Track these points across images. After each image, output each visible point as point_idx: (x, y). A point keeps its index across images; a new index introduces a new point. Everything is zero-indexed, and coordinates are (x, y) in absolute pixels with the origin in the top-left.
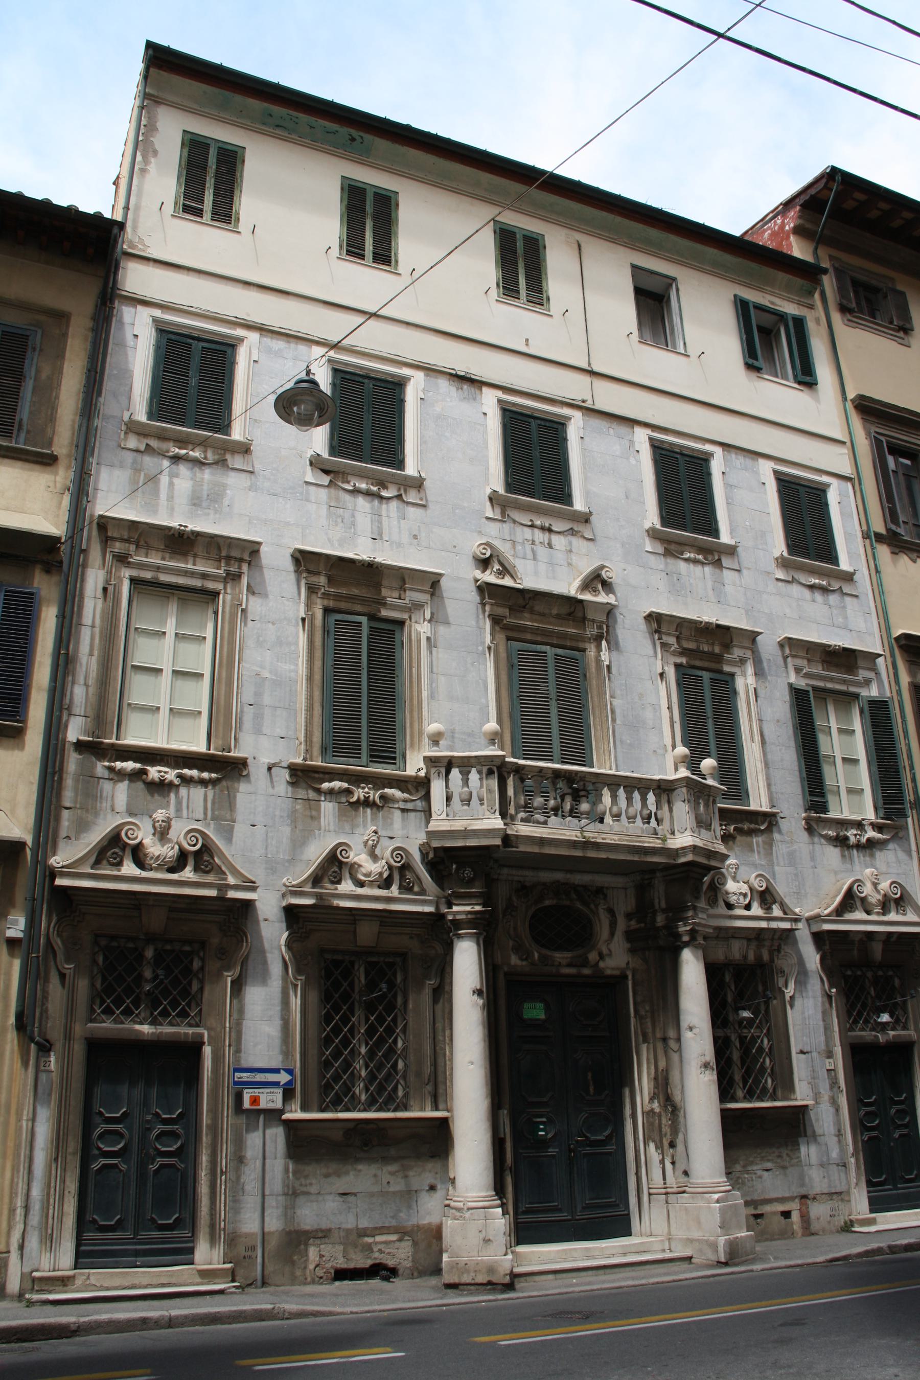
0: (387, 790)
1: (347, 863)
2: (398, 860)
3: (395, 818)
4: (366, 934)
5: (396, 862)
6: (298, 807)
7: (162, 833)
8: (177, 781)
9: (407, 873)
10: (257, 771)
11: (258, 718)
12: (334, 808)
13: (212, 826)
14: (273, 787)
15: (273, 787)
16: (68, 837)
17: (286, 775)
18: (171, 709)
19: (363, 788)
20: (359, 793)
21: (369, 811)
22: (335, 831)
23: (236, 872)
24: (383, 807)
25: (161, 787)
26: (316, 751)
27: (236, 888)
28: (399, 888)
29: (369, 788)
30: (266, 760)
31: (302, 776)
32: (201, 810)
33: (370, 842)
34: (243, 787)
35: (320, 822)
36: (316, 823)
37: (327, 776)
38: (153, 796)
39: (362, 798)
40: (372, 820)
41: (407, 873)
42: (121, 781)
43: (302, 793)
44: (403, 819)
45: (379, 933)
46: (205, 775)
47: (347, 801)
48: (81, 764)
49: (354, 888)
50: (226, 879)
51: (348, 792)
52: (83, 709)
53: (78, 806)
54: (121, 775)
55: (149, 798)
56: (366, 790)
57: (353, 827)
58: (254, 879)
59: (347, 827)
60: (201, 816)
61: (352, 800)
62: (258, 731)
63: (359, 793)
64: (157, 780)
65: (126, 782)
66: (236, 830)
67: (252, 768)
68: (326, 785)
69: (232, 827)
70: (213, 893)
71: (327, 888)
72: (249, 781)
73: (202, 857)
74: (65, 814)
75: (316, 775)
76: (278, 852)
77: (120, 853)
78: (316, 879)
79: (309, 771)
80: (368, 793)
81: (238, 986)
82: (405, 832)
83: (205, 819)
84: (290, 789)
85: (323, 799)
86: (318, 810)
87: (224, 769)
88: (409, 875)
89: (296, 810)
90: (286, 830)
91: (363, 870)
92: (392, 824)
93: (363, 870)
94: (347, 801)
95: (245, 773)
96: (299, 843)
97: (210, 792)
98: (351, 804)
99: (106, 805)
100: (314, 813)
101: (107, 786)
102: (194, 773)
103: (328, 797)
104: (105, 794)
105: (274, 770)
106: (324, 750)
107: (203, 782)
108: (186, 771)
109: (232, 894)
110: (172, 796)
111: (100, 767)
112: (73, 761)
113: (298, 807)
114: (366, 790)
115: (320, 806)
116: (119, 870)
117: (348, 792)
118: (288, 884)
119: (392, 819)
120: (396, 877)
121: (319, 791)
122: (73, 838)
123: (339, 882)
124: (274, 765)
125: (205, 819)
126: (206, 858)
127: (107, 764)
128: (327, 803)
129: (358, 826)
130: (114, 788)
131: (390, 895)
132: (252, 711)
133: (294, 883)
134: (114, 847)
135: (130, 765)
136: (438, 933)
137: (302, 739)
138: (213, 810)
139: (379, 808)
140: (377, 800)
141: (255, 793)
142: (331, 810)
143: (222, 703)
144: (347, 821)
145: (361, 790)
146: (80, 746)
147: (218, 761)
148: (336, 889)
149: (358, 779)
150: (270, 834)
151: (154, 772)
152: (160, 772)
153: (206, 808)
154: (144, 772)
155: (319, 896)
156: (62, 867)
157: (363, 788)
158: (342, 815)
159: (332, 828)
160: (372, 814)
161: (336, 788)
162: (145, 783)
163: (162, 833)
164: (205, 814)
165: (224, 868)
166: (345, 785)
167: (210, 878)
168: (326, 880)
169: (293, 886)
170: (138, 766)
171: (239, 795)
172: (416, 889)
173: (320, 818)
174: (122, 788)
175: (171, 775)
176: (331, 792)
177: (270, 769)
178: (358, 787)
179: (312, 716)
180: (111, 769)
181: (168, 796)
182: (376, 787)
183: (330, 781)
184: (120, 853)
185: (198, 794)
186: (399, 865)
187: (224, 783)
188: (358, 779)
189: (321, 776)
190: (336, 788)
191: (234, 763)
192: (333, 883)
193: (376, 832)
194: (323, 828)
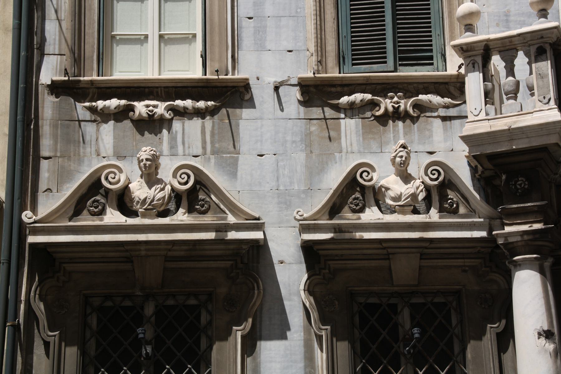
0: (421, 97)
1: (369, 187)
2: (435, 176)
4: (404, 269)
5: (431, 180)
7: (151, 176)
8: (167, 116)
9: (449, 192)
10: (262, 94)
11: (260, 32)
12: (357, 125)
13: (213, 161)
14: (282, 110)
15: (282, 110)
16: (49, 190)
17: (296, 94)
18: (161, 37)
19: (392, 98)
20: (387, 104)
21: (400, 124)
22: (359, 152)
23: (235, 210)
24: (418, 117)
25: (151, 125)
26: (331, 60)
27: (237, 227)
28: (440, 211)
30: (272, 79)
31: (316, 93)
32: (199, 144)
33: (398, 159)
34: (246, 113)
35: (340, 143)
36: (335, 144)
38: (143, 135)
39: (390, 109)
41: (449, 192)
42: (106, 122)
43: (316, 112)
44: (445, 129)
45: (420, 268)
46: (201, 104)
47: (373, 115)
48: (58, 108)
49: (380, 215)
50: (225, 219)
51: (374, 105)
52: (57, 47)
53: (58, 154)
54: (104, 116)
55: (138, 136)
58: (257, 216)
59: (374, 146)
60: (199, 151)
61: (378, 114)
62: (261, 47)
63: (387, 104)
64: (145, 115)
65: (112, 123)
66: (240, 162)
67: (256, 91)
68: (345, 100)
69: (237, 160)
70: (211, 235)
71: (348, 217)
72: (254, 106)
73: (196, 194)
74: (44, 164)
75: (333, 89)
76: (291, 183)
77: (103, 201)
78: (334, 208)
79: (324, 86)
80: (398, 103)
81: (250, 346)
82: (448, 144)
83: (205, 153)
84: (302, 109)
85: (343, 116)
86: (338, 129)
87: (226, 95)
88: (451, 195)
89: (311, 133)
90: (300, 157)
91: (391, 193)
92: (431, 136)
93: (391, 193)
94: (373, 115)
95: (247, 97)
96: (315, 171)
97: (208, 122)
98: (377, 118)
99: (90, 150)
101: (90, 129)
102: (188, 103)
103: (349, 113)
104: (87, 138)
105: (281, 90)
106: (341, 60)
107: (200, 113)
108: (179, 103)
109: (232, 235)
110: (165, 132)
111: (81, 109)
112: (48, 105)
116: (102, 220)
117: (374, 105)
118: (298, 217)
119: (430, 130)
120: (435, 198)
121: (337, 108)
122: (55, 190)
123: (362, 210)
124: (282, 83)
125: (205, 153)
126: (201, 196)
127: (87, 104)
128: (348, 120)
129: (387, 143)
130: (98, 130)
131: (428, 220)
132: (252, 25)
133: (305, 215)
134: (93, 194)
135: (114, 103)
136: (493, 264)
137: (312, 49)
138: (212, 143)
139: (414, 120)
141: (261, 119)
142: (353, 128)
143: (216, 20)
144: (374, 139)
145: (388, 101)
146: (56, 88)
147: (216, 87)
148: (359, 218)
149: (383, 88)
150: (281, 164)
151: (141, 108)
152: (148, 106)
153: (204, 142)
154: (131, 109)
155: (338, 229)
156: (35, 222)
158: (366, 132)
159: (355, 148)
161: (358, 101)
162: (132, 121)
163: (151, 176)
164: (204, 148)
165: (222, 206)
166: (368, 96)
167: (207, 219)
168: (346, 208)
169: (305, 219)
170: (123, 102)
171: (242, 123)
172: (462, 210)
173: (340, 138)
174: (108, 130)
175: (161, 108)
176: (352, 105)
177: (276, 89)
178: (385, 97)
180: (93, 110)
181: (160, 132)
182: (407, 96)
183: (349, 95)
184: (103, 201)
185: (194, 125)
186: (436, 183)
187: (224, 111)
188: (383, 88)
189: (339, 89)
191: (234, 87)
192: (354, 211)
193: (404, 147)
194: (344, 150)
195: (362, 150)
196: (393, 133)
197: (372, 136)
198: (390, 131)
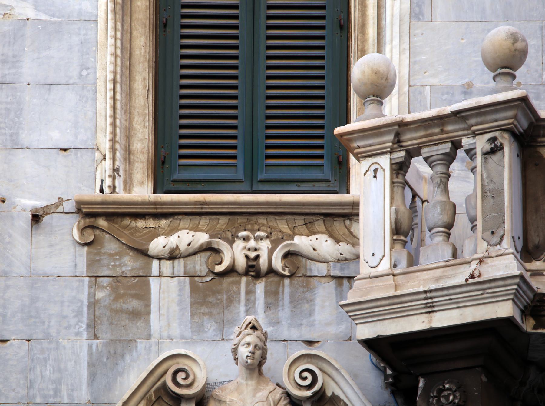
3: (318, 301)
6: (100, 295)
20: (235, 253)
22: (183, 338)
26: (142, 171)
29: (257, 239)
35: (148, 322)
36: (140, 324)
37: (164, 223)
39: (241, 263)
40: (268, 306)
47: (211, 272)
56: (252, 243)
57: (223, 325)
59: (211, 328)
61: (219, 269)
92: (311, 313)
94: (211, 272)
100: (134, 304)
113: (100, 295)
114: (252, 243)
115: (148, 285)
129: (233, 322)
140: (278, 264)
144: (210, 314)
157: (246, 239)
160: (267, 293)
173: (149, 313)
179: (129, 94)
183: (169, 233)
189: (151, 223)
190: (183, 247)
195: (188, 334)
196: (246, 305)
197: (207, 310)
198: (239, 302)
